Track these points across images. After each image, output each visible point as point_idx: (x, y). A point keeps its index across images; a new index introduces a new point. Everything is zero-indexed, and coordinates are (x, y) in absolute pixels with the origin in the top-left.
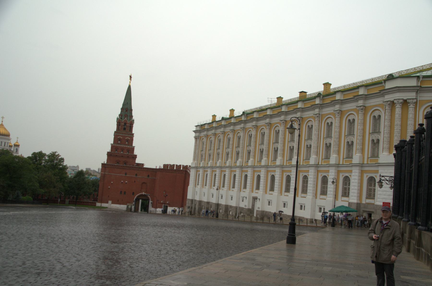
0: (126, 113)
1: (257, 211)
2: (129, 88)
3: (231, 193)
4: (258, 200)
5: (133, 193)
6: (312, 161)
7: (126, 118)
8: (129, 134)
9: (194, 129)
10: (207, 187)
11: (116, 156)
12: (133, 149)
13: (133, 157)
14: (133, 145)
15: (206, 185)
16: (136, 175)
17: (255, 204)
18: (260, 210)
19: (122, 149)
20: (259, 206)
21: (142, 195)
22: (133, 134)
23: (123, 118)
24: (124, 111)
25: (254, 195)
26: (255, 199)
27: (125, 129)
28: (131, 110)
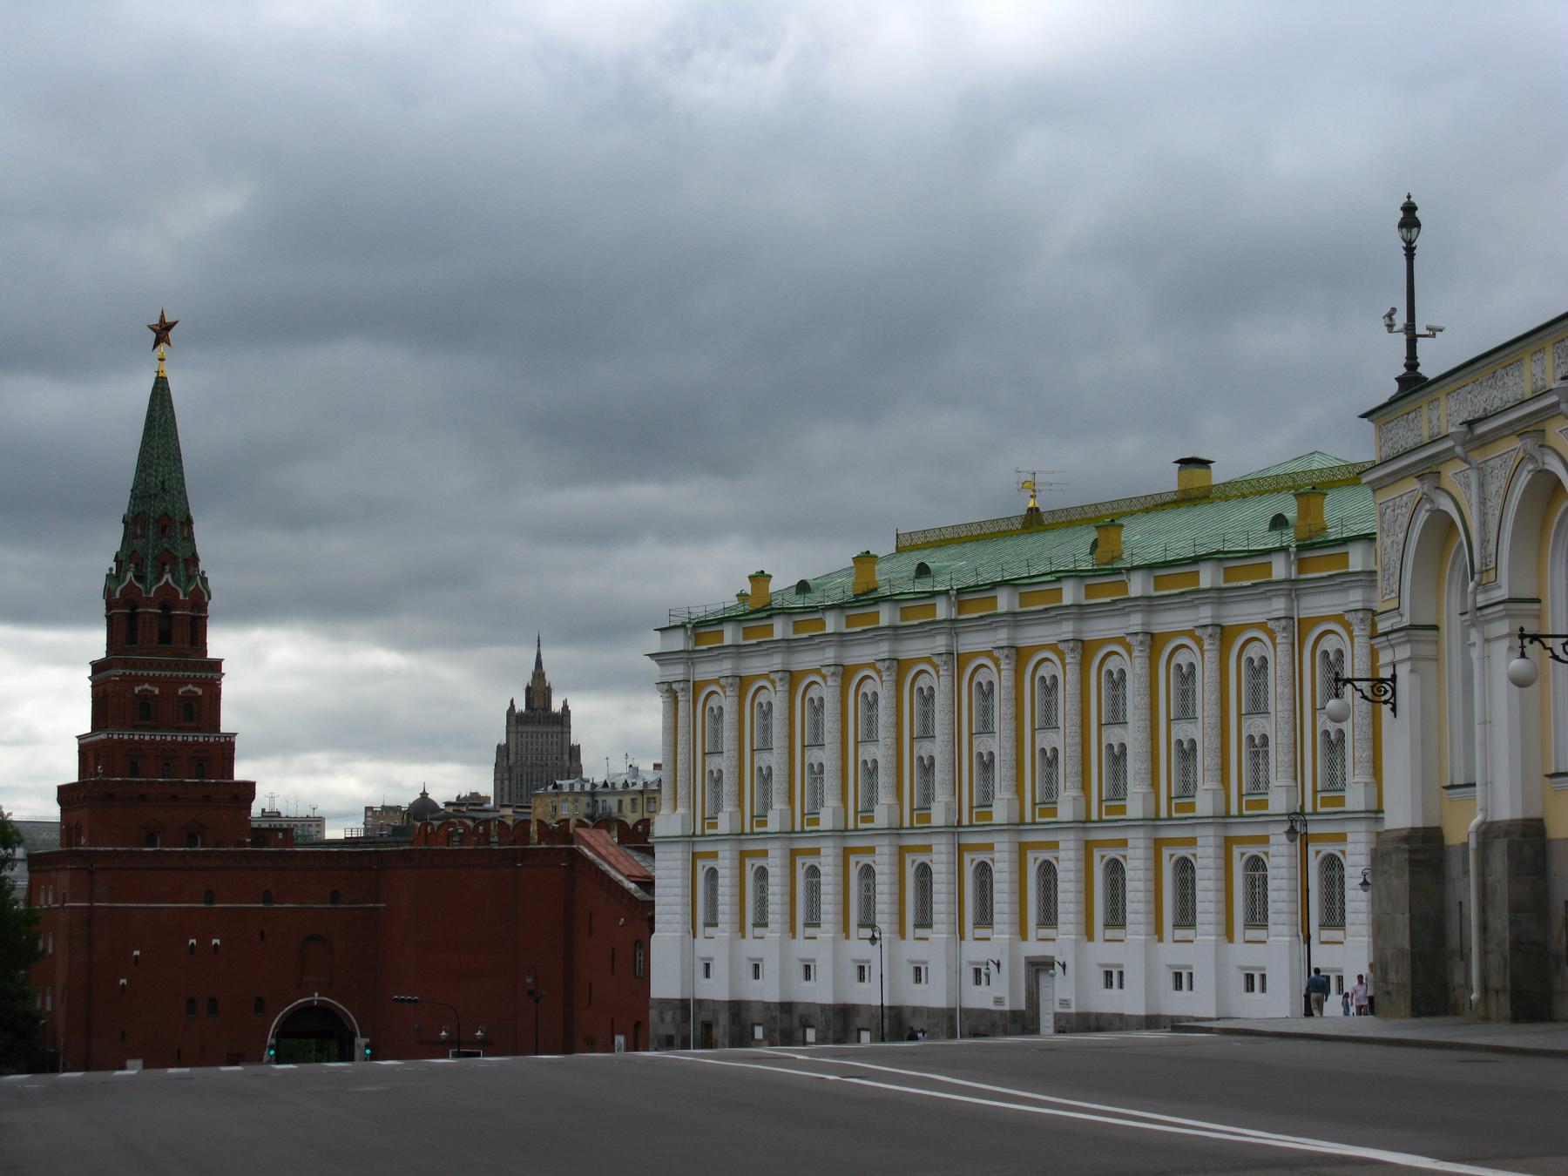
0: (165, 543)
1: (1058, 1017)
2: (161, 392)
3: (752, 947)
4: (1058, 968)
5: (260, 1004)
6: (1279, 802)
7: (167, 577)
8: (186, 667)
9: (656, 643)
10: (724, 930)
11: (142, 796)
12: (225, 751)
13: (235, 798)
14: (226, 726)
15: (712, 922)
16: (267, 897)
17: (1043, 991)
18: (1073, 1010)
19: (168, 756)
20: (1060, 994)
21: (308, 1009)
22: (216, 665)
23: (150, 577)
24: (152, 532)
25: (1034, 948)
26: (1040, 967)
27: (165, 637)
28: (188, 522)
